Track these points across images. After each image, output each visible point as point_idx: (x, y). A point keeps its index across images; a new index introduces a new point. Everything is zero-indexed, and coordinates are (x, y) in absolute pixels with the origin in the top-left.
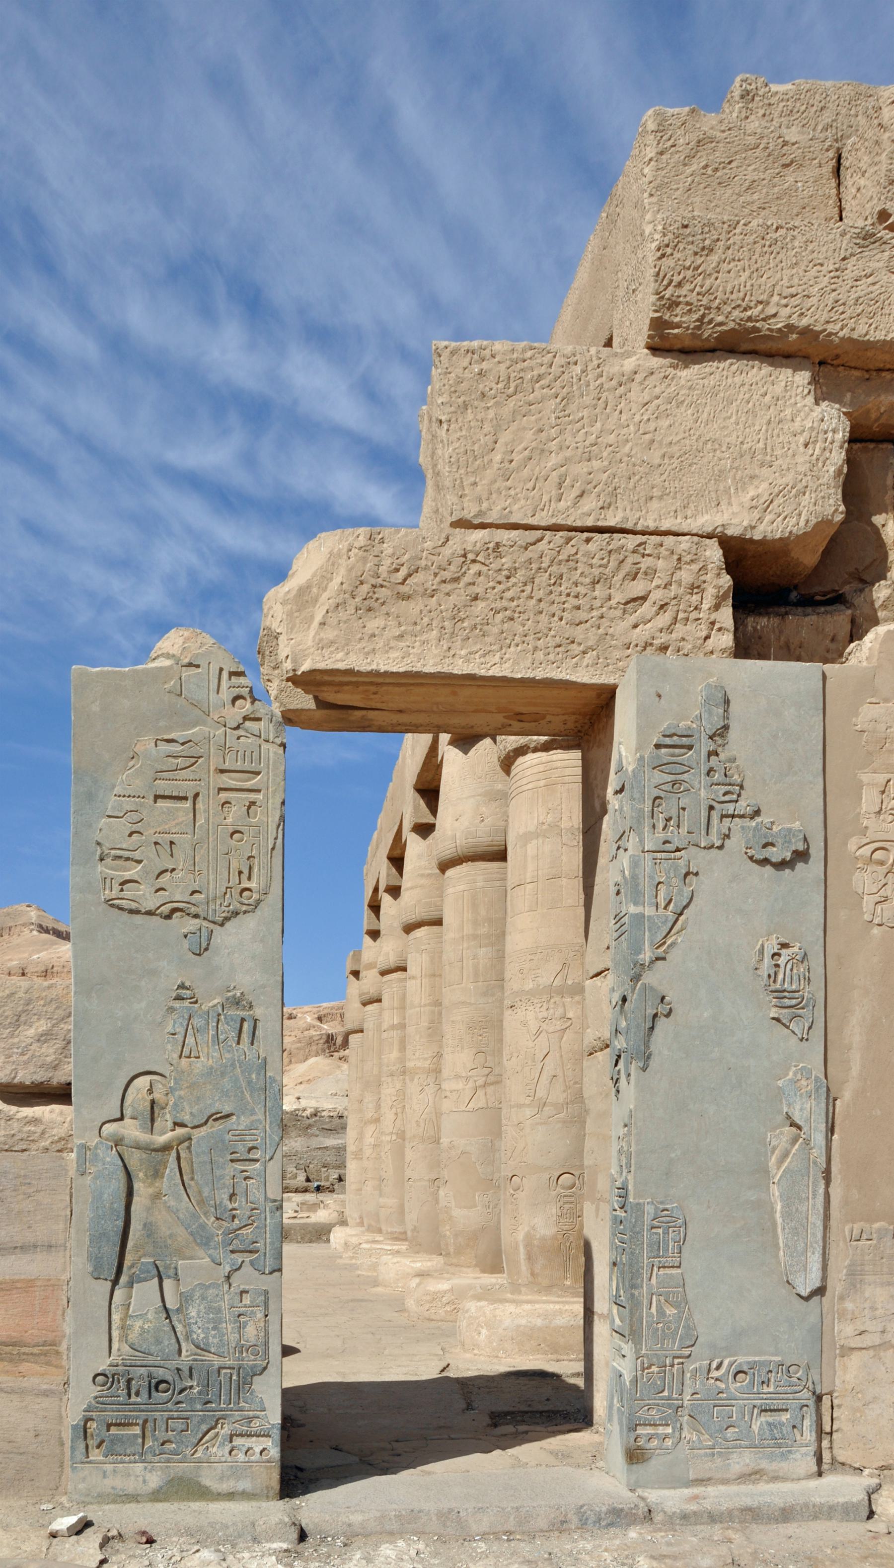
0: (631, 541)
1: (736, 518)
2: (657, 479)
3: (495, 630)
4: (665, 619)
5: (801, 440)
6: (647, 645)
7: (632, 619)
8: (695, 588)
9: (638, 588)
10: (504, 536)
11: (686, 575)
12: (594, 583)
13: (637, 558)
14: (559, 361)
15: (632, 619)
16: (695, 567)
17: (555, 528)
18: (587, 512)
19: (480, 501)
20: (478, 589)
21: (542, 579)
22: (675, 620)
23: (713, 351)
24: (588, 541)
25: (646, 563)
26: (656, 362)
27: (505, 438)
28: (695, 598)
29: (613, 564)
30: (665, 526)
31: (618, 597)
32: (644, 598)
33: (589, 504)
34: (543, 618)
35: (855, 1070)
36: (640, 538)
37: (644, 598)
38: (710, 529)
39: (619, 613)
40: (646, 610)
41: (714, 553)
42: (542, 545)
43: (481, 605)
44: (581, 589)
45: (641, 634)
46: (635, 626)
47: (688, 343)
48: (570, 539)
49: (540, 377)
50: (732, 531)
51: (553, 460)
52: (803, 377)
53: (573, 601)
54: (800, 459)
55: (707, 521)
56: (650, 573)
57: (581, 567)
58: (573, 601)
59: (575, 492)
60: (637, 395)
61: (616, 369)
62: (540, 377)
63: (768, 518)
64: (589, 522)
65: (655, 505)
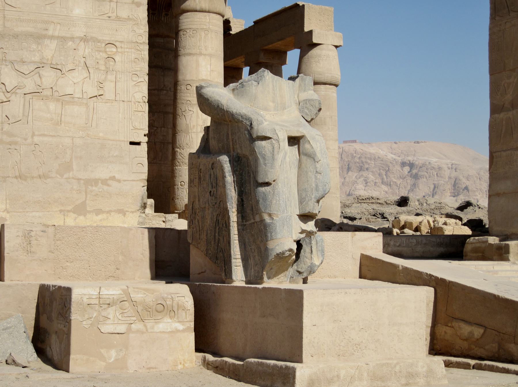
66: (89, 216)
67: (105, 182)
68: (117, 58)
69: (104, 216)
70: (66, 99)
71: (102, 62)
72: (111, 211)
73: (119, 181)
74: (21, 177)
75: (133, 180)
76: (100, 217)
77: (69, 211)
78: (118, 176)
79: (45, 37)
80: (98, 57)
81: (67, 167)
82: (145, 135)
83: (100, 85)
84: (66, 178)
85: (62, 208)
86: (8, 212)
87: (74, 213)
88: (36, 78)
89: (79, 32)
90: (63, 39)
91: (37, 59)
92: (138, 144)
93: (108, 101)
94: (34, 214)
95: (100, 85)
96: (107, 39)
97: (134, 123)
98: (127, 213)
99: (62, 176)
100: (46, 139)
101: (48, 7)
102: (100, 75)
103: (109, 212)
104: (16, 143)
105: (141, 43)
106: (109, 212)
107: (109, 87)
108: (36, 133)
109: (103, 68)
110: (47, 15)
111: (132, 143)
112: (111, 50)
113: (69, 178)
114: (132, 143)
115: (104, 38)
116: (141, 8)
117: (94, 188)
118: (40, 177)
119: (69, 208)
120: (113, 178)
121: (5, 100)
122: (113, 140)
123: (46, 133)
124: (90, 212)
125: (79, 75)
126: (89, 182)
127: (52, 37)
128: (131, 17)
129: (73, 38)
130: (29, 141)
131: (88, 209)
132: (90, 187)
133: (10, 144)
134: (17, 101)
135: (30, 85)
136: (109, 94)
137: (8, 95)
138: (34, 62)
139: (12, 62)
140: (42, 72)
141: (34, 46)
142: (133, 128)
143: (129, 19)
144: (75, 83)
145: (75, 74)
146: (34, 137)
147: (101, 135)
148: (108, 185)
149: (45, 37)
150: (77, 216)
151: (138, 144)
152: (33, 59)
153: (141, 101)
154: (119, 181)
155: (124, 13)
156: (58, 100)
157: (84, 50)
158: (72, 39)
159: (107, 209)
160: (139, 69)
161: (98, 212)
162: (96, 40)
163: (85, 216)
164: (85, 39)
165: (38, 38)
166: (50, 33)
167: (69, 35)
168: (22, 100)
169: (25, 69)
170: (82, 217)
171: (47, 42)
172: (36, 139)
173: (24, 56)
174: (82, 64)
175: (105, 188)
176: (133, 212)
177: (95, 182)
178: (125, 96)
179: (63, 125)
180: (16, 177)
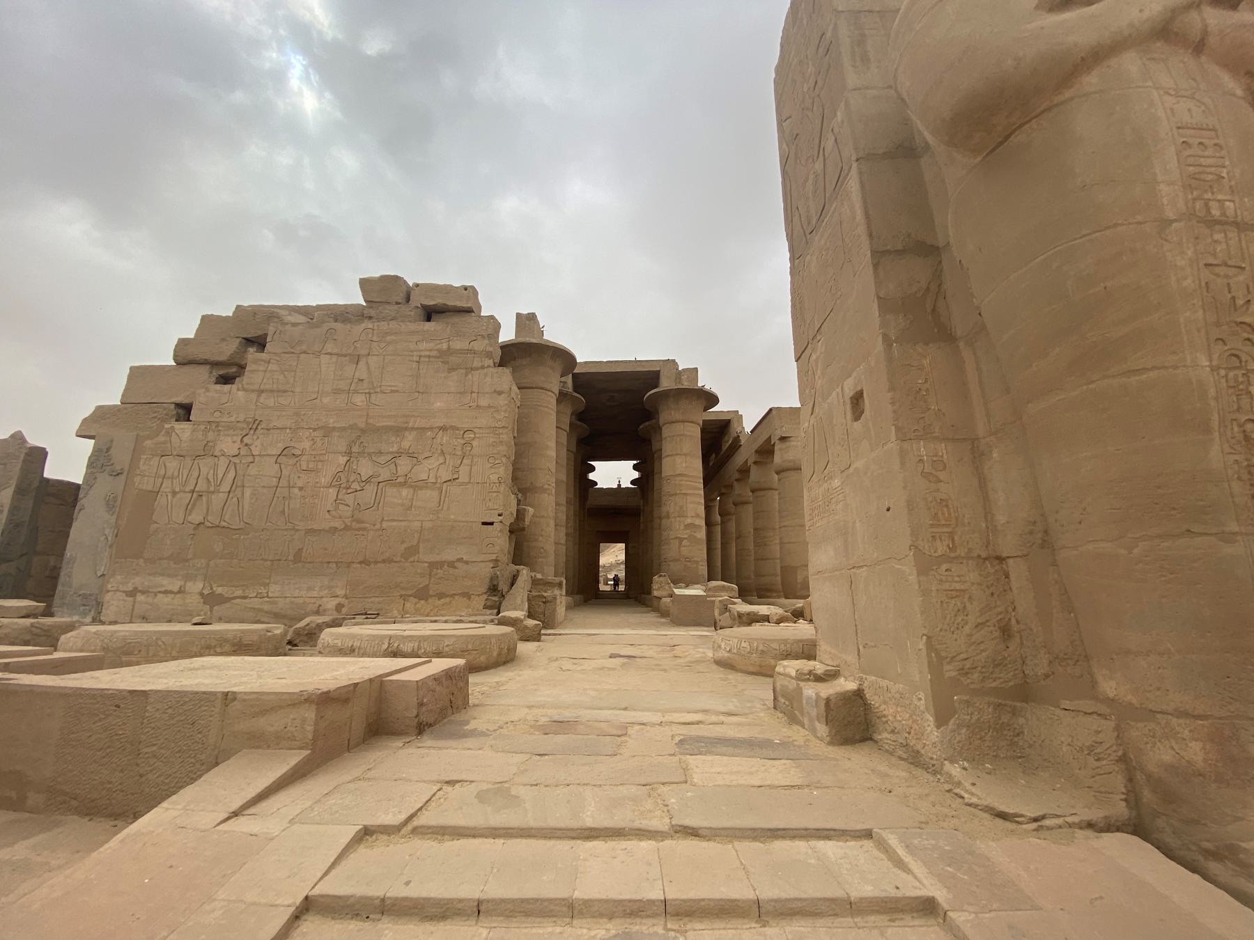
66: (430, 600)
67: (452, 565)
68: (475, 443)
69: (448, 600)
70: (418, 485)
74: (365, 562)
76: (443, 601)
78: (465, 558)
79: (406, 429)
81: (412, 551)
83: (456, 469)
89: (439, 422)
90: (424, 429)
91: (395, 449)
92: (492, 524)
95: (456, 469)
96: (466, 426)
99: (406, 559)
103: (453, 596)
104: (364, 529)
106: (453, 596)
107: (464, 470)
109: (459, 453)
111: (484, 524)
114: (484, 524)
118: (384, 561)
119: (410, 592)
120: (460, 560)
125: (433, 463)
126: (434, 565)
127: (412, 429)
130: (378, 526)
133: (359, 529)
134: (370, 490)
135: (385, 474)
136: (463, 478)
139: (370, 454)
143: (489, 407)
144: (428, 469)
145: (431, 460)
149: (406, 429)
151: (492, 524)
154: (467, 563)
155: (484, 402)
156: (411, 486)
157: (444, 438)
158: (431, 429)
161: (441, 596)
162: (454, 428)
164: (443, 428)
165: (399, 431)
166: (411, 425)
169: (382, 459)
171: (407, 433)
172: (385, 525)
175: (451, 571)
177: (440, 564)
180: (361, 563)
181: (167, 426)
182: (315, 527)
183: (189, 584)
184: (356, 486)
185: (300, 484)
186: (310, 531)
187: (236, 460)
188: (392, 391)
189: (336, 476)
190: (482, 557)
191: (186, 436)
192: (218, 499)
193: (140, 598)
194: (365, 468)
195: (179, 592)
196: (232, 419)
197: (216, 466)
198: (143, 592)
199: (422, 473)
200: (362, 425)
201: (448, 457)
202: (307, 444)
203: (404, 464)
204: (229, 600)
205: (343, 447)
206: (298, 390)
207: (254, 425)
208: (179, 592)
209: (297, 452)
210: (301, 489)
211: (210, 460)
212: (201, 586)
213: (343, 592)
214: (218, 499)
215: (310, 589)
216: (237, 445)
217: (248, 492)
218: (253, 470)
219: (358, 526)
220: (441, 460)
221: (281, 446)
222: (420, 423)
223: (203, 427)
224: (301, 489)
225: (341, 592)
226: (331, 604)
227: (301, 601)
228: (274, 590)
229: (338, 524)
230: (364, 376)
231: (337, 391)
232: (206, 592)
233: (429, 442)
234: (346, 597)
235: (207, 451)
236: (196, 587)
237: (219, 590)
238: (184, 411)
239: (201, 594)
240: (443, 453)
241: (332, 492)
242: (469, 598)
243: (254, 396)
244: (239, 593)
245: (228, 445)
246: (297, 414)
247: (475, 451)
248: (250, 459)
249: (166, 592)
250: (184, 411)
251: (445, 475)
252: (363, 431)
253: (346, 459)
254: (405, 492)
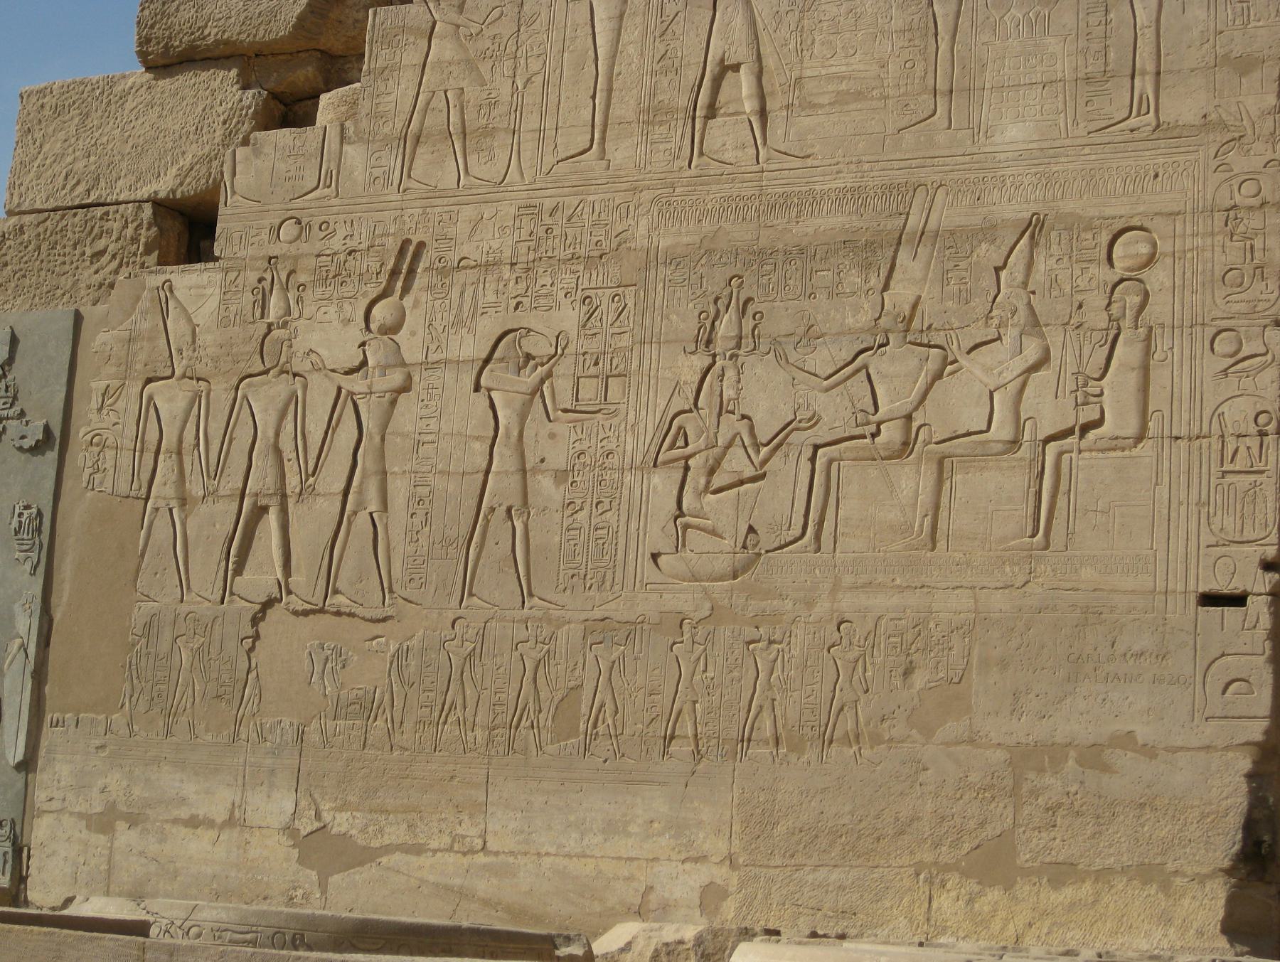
0: (99, 211)
1: (163, 186)
2: (123, 165)
3: (13, 285)
4: (115, 264)
5: (222, 118)
6: (101, 285)
7: (95, 266)
8: (135, 240)
9: (101, 244)
10: (27, 219)
11: (129, 232)
12: (75, 246)
13: (103, 223)
14: (89, 88)
15: (95, 266)
16: (135, 224)
17: (54, 210)
18: (77, 196)
19: (21, 196)
20: (8, 258)
21: (44, 247)
22: (120, 265)
23: (181, 63)
24: (75, 215)
25: (107, 225)
26: (149, 76)
27: (46, 147)
28: (135, 246)
29: (88, 228)
30: (121, 198)
31: (89, 252)
32: (102, 253)
33: (81, 189)
34: (43, 273)
35: (65, 599)
36: (105, 209)
37: (102, 253)
38: (146, 196)
39: (88, 263)
40: (107, 257)
41: (148, 210)
42: (48, 222)
43: (9, 267)
44: (67, 250)
45: (97, 278)
46: (96, 272)
47: (161, 62)
48: (63, 217)
49: (74, 103)
50: (162, 195)
51: (69, 159)
52: (234, 73)
53: (61, 259)
54: (218, 133)
55: (144, 192)
56: (109, 232)
57: (69, 234)
58: (61, 259)
59: (74, 182)
60: (129, 106)
61: (120, 88)
62: (74, 103)
63: (188, 180)
64: (77, 202)
65: (120, 183)
66: (1023, 889)
67: (1094, 757)
68: (1157, 278)
69: (1087, 888)
71: (1097, 300)
72: (1109, 870)
73: (1149, 751)
75: (1208, 748)
76: (1068, 893)
77: (947, 868)
78: (1144, 733)
80: (1082, 283)
82: (1268, 566)
84: (947, 744)
85: (928, 857)
86: (733, 866)
87: (965, 874)
88: (858, 386)
92: (1238, 600)
93: (1115, 444)
94: (822, 874)
95: (1087, 388)
96: (1120, 209)
97: (1216, 522)
98: (1178, 881)
99: (928, 732)
100: (882, 602)
101: (908, 136)
102: (1086, 351)
105: (1251, 208)
106: (1103, 875)
108: (848, 580)
110: (903, 164)
111: (1210, 600)
112: (1132, 250)
113: (958, 743)
114: (1210, 600)
115: (1109, 212)
116: (1256, 75)
117: (1048, 780)
120: (1126, 741)
121: (749, 472)
122: (1133, 592)
123: (880, 578)
124: (1027, 873)
128: (1213, 116)
129: (994, 227)
131: (1023, 858)
132: (1031, 775)
134: (788, 473)
135: (835, 412)
137: (764, 450)
138: (851, 332)
139: (775, 341)
140: (877, 364)
141: (854, 278)
142: (1213, 540)
143: (1207, 125)
146: (840, 596)
147: (1087, 573)
148: (1106, 768)
150: (976, 888)
151: (1238, 600)
152: (850, 321)
153: (1253, 429)
154: (1149, 751)
155: (1183, 106)
158: (988, 232)
159: (1098, 864)
160: (1243, 307)
161: (1061, 874)
162: (1076, 226)
163: (1008, 887)
164: (1034, 228)
167: (976, 221)
168: (805, 466)
170: (994, 894)
172: (847, 603)
173: (819, 317)
174: (1022, 312)
176: (1202, 879)
178: (1185, 416)
179: (941, 544)
181: (155, 280)
182: (618, 610)
183: (256, 800)
184: (737, 463)
185: (558, 458)
186: (599, 630)
187: (356, 384)
188: (841, 99)
189: (673, 433)
190: (1209, 732)
191: (205, 313)
192: (312, 521)
193: (126, 836)
194: (765, 394)
195: (230, 822)
196: (336, 243)
197: (293, 405)
198: (133, 821)
199: (961, 404)
200: (740, 233)
201: (1055, 338)
202: (568, 317)
203: (896, 375)
204: (367, 856)
205: (684, 321)
206: (531, 121)
207: (405, 265)
208: (230, 822)
209: (540, 347)
210: (561, 476)
211: (279, 388)
212: (289, 807)
213: (722, 846)
214: (312, 521)
215: (611, 828)
216: (356, 333)
217: (399, 489)
218: (408, 414)
219: (755, 606)
220: (1032, 352)
221: (489, 327)
222: (947, 214)
223: (253, 277)
224: (561, 476)
225: (720, 846)
226: (682, 884)
227: (585, 868)
228: (502, 829)
229: (684, 599)
230: (740, 52)
231: (651, 115)
232: (306, 825)
233: (988, 281)
234: (731, 860)
235: (271, 355)
236: (274, 806)
237: (342, 822)
238: (189, 229)
239: (289, 830)
240: (1034, 324)
241: (662, 484)
242: (1165, 887)
243: (391, 160)
244: (396, 833)
245: (328, 334)
246: (529, 209)
247: (1158, 310)
248: (396, 378)
249: (193, 823)
250: (189, 229)
251: (1048, 409)
252: (760, 256)
253: (700, 361)
254: (912, 480)
